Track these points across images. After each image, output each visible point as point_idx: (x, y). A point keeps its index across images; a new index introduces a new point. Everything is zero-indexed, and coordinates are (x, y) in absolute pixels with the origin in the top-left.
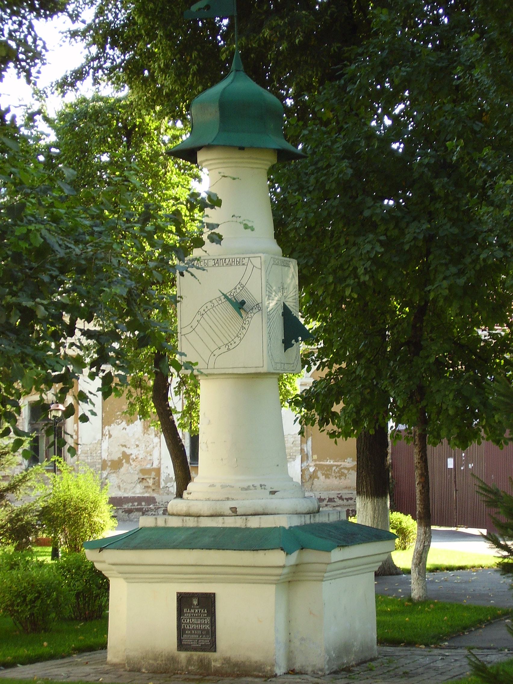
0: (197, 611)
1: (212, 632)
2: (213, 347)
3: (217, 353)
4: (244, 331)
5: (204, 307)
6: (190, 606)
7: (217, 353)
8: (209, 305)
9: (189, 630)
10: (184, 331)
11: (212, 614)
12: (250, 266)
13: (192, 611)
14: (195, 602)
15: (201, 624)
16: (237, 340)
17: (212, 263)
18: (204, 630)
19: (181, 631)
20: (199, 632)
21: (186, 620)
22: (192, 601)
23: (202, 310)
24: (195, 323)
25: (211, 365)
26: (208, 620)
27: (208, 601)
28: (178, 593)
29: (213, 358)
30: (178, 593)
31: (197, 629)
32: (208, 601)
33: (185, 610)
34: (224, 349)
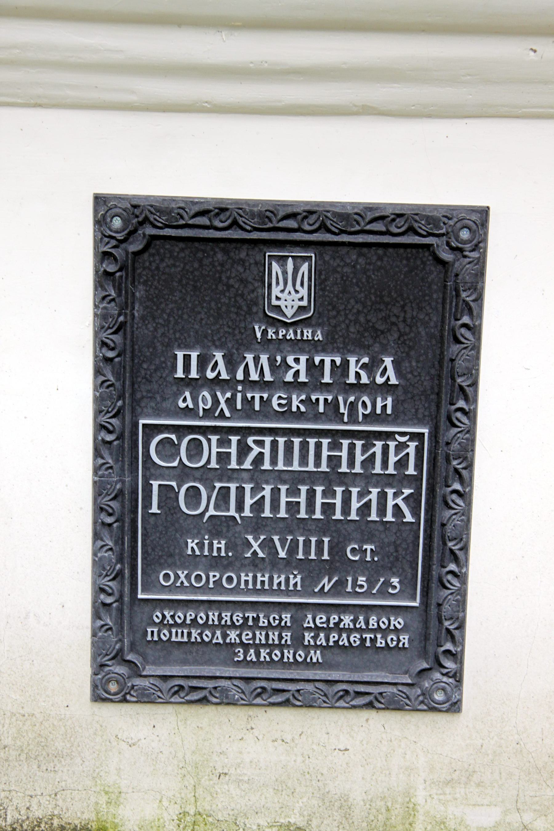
0: (298, 366)
1: (431, 551)
6: (235, 315)
9: (219, 527)
11: (442, 392)
13: (256, 365)
14: (289, 290)
15: (333, 478)
18: (364, 530)
19: (132, 533)
20: (315, 548)
22: (262, 280)
26: (404, 445)
27: (408, 284)
28: (99, 200)
30: (99, 200)
31: (293, 525)
32: (408, 284)
33: (185, 361)
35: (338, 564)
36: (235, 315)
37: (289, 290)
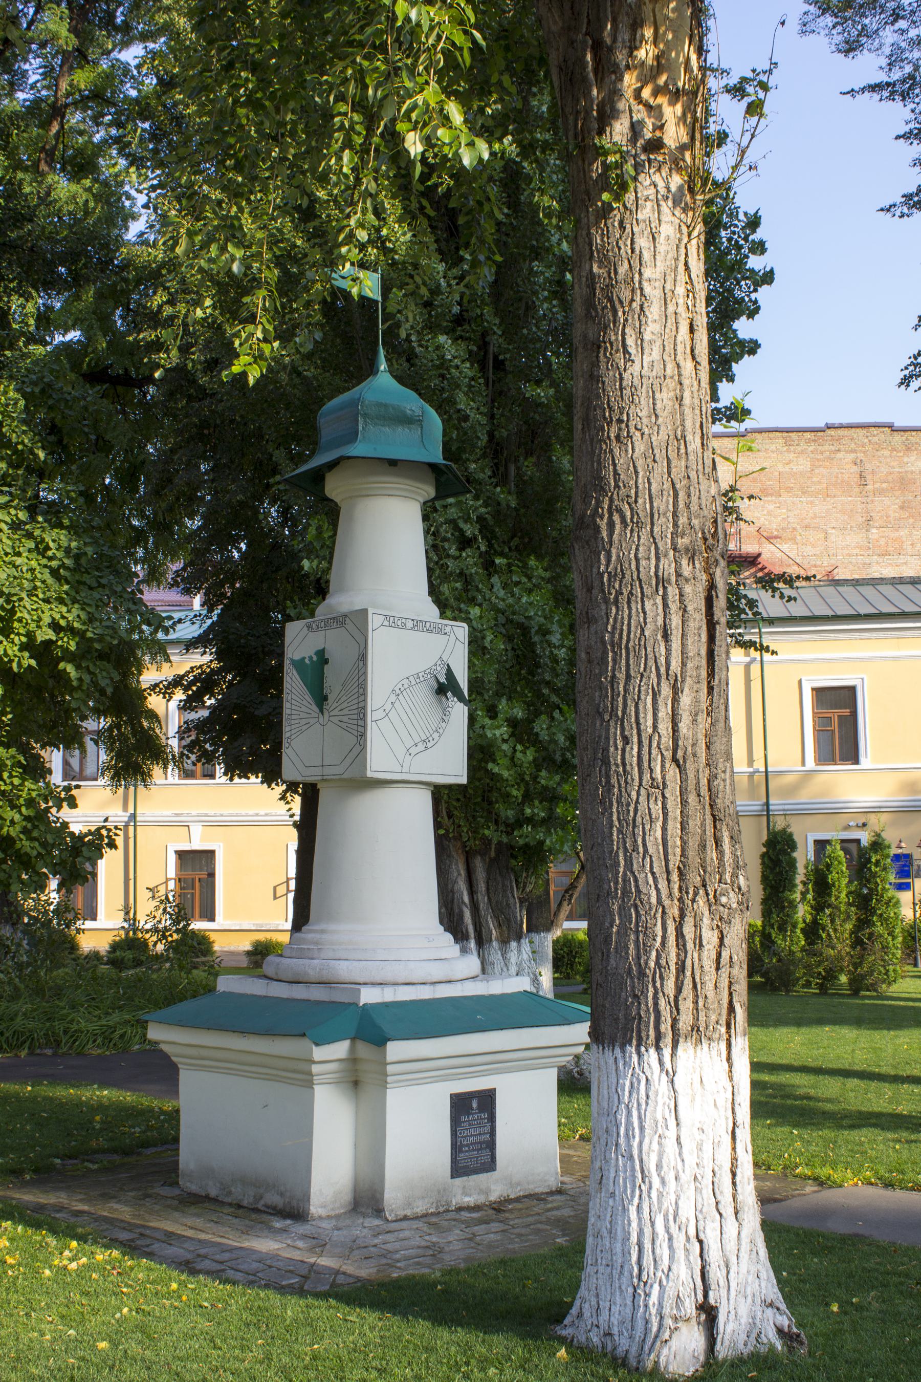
1: (491, 1145)
2: (409, 743)
3: (414, 751)
4: (444, 725)
5: (400, 686)
6: (468, 1110)
7: (414, 751)
8: (406, 682)
9: (467, 1145)
10: (376, 715)
12: (453, 637)
13: (471, 1118)
14: (475, 1105)
16: (436, 735)
17: (410, 624)
18: (484, 1142)
19: (456, 1148)
20: (478, 1146)
21: (463, 1132)
23: (397, 689)
24: (388, 707)
25: (405, 769)
29: (408, 758)
34: (421, 747)
35: (481, 1149)
36: (468, 1110)
37: (475, 1105)
